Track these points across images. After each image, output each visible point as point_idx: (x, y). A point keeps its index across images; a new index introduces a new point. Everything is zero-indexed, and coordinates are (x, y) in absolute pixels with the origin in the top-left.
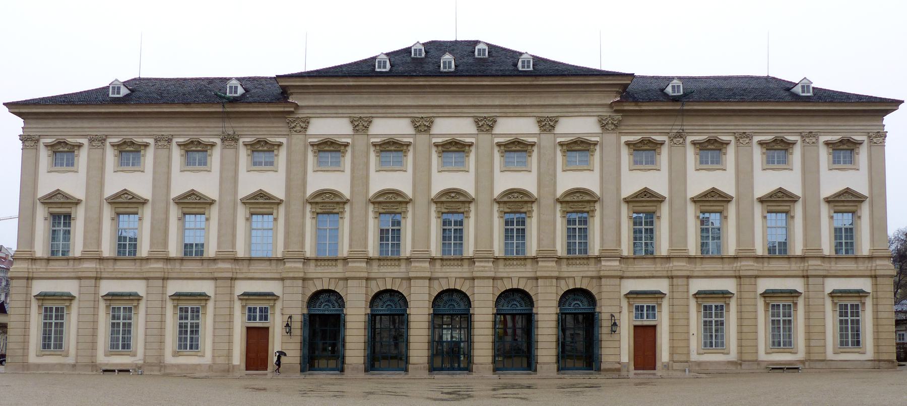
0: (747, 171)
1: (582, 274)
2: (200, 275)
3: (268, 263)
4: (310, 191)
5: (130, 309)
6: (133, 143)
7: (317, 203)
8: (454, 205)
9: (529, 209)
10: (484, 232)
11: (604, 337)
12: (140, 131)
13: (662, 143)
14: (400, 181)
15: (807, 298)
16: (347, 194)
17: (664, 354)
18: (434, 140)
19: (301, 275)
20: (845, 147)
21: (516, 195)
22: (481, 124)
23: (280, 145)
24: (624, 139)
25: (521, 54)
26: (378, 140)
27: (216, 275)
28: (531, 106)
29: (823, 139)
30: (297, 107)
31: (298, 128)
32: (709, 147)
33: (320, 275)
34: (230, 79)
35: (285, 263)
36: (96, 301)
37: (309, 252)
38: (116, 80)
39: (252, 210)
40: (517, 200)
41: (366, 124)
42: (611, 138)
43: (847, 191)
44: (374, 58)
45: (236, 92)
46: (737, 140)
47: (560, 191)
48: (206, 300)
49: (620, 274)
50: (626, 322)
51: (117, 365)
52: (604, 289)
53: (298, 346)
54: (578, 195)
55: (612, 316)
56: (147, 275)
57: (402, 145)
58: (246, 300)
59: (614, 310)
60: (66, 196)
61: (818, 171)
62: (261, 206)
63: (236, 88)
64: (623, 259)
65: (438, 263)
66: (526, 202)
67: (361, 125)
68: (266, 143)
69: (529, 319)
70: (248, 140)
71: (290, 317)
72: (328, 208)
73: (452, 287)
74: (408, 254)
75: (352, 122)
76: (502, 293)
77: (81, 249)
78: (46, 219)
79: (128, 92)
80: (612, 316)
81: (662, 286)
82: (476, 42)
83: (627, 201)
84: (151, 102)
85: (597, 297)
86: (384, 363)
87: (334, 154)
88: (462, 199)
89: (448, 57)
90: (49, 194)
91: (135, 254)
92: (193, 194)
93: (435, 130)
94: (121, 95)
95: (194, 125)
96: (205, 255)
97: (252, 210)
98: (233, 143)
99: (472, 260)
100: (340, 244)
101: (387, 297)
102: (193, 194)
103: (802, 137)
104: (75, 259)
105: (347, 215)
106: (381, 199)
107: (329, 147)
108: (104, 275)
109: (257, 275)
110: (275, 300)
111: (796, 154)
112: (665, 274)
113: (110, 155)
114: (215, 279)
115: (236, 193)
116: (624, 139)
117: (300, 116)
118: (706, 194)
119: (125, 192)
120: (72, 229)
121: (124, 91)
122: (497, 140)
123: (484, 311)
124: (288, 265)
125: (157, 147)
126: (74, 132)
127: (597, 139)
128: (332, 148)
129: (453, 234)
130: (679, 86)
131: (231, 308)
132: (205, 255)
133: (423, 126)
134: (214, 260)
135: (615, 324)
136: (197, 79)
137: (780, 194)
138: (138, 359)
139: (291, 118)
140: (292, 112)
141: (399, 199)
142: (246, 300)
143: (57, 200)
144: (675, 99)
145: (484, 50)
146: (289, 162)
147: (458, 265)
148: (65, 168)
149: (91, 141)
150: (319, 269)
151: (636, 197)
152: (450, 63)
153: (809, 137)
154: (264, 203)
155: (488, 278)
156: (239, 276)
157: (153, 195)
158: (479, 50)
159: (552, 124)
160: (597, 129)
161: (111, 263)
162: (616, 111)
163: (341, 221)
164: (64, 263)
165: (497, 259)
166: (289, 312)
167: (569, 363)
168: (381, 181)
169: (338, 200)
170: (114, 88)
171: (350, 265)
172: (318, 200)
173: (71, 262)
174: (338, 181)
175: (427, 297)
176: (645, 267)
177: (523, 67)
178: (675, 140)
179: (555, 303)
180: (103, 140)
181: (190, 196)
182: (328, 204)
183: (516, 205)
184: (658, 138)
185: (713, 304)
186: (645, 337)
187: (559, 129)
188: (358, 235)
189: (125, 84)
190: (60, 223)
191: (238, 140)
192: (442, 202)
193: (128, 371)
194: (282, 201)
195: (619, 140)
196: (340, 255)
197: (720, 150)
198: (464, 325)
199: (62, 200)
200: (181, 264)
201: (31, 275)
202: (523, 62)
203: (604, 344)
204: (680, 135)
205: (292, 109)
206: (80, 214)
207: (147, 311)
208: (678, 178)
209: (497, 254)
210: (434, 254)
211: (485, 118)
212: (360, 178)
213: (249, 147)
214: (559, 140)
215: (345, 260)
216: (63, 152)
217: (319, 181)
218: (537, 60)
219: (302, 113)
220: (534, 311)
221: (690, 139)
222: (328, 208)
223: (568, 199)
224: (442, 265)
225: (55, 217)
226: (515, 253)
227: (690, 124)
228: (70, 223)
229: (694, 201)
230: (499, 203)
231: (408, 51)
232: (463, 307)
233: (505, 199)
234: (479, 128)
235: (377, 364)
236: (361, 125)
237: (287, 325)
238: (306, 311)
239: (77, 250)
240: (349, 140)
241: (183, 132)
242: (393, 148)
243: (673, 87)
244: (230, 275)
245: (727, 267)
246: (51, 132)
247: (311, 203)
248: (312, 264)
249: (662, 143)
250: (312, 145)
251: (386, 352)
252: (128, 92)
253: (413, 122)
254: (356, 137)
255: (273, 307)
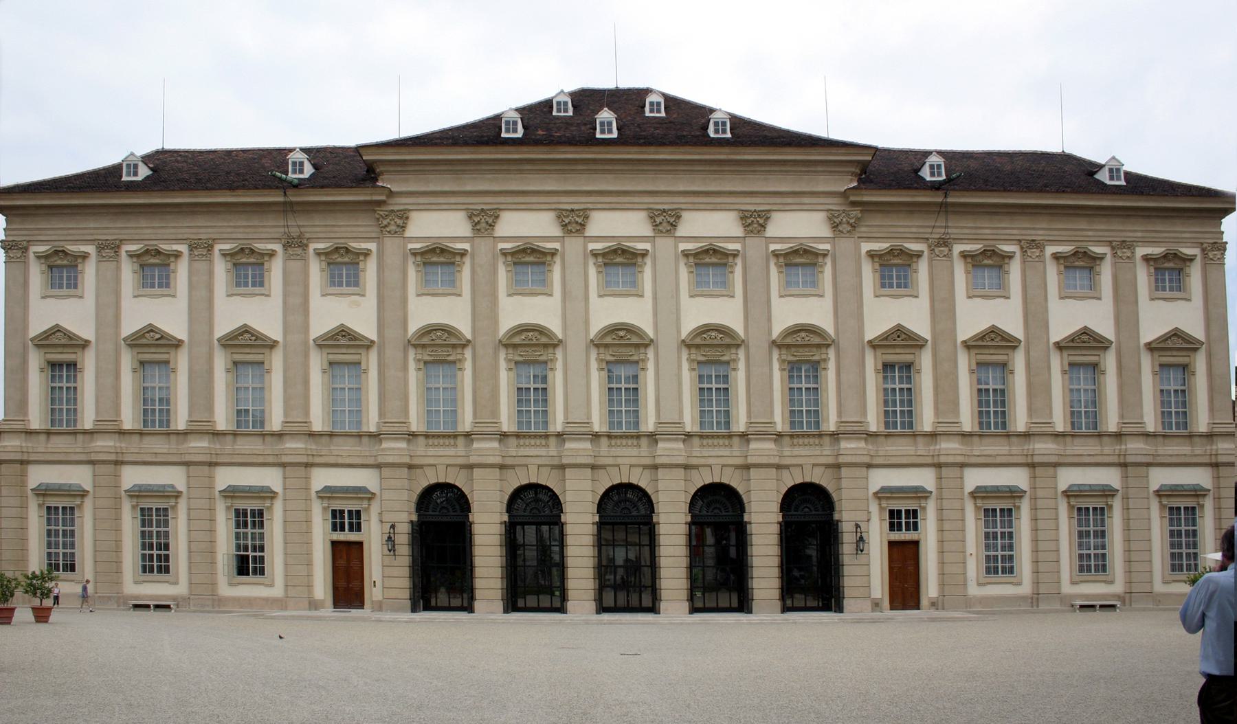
0: (1039, 301)
1: (813, 461)
2: (261, 460)
3: (357, 439)
4: (413, 327)
5: (166, 510)
6: (158, 252)
7: (424, 346)
8: (622, 350)
9: (733, 356)
10: (668, 394)
11: (846, 559)
12: (171, 236)
13: (919, 255)
14: (542, 310)
15: (1126, 498)
16: (466, 330)
17: (930, 588)
18: (592, 246)
19: (407, 460)
20: (1171, 265)
21: (713, 334)
22: (658, 220)
23: (367, 254)
24: (866, 247)
25: (712, 111)
26: (508, 245)
27: (285, 459)
28: (731, 193)
29: (1141, 251)
30: (391, 194)
31: (393, 228)
32: (986, 262)
33: (432, 461)
34: (291, 150)
35: (381, 441)
36: (118, 499)
37: (416, 423)
38: (132, 154)
39: (331, 357)
40: (715, 342)
41: (490, 221)
42: (845, 244)
43: (1176, 334)
44: (498, 118)
45: (301, 171)
46: (1024, 251)
47: (777, 330)
48: (272, 498)
49: (866, 460)
50: (878, 536)
51: (152, 597)
52: (844, 483)
53: (406, 572)
54: (803, 334)
55: (857, 526)
56: (188, 458)
57: (544, 254)
58: (329, 498)
59: (860, 516)
60: (69, 336)
61: (1136, 302)
62: (344, 351)
63: (302, 164)
64: (871, 436)
65: (604, 441)
66: (729, 346)
67: (483, 222)
68: (347, 250)
69: (741, 531)
70: (321, 246)
71: (393, 527)
72: (441, 353)
73: (625, 481)
74: (559, 428)
75: (470, 217)
76: (699, 490)
77: (93, 417)
78: (42, 370)
79: (149, 172)
80: (857, 526)
81: (924, 478)
82: (647, 91)
83: (873, 345)
84: (185, 185)
85: (835, 496)
86: (531, 601)
87: (446, 269)
88: (635, 340)
89: (606, 115)
90: (45, 332)
91: (168, 426)
92: (247, 332)
93: (593, 229)
94: (140, 178)
95: (245, 224)
96: (267, 428)
97: (331, 357)
98: (299, 251)
99: (653, 437)
100: (459, 411)
101: (531, 494)
102: (247, 332)
103: (1113, 248)
104: (85, 432)
105: (468, 365)
106: (517, 340)
107: (439, 258)
108: (127, 458)
109: (340, 461)
110: (370, 499)
111: (1106, 273)
112: (929, 460)
113: (128, 272)
114: (283, 465)
115: (306, 328)
116: (866, 247)
117: (396, 208)
118: (982, 336)
119: (151, 329)
120: (79, 385)
121: (144, 172)
122: (683, 246)
123: (674, 518)
124: (385, 445)
125: (192, 259)
126: (79, 237)
127: (827, 247)
128: (442, 259)
129: (623, 395)
130: (939, 166)
131: (308, 511)
132: (267, 428)
133: (573, 223)
134: (280, 435)
135: (861, 539)
136: (244, 151)
137: (1085, 337)
138: (181, 589)
139: (381, 211)
140: (380, 203)
141: (544, 340)
142: (329, 498)
143: (57, 342)
144: (936, 187)
145: (659, 104)
146: (381, 283)
147: (633, 446)
148: (65, 291)
149: (100, 248)
150: (431, 452)
151: (886, 339)
152: (610, 124)
153: (1122, 247)
154: (348, 346)
155: (677, 466)
156: (318, 460)
157: (191, 333)
158: (652, 104)
159: (761, 221)
160: (826, 232)
161: (136, 438)
162: (854, 204)
163: (459, 373)
164: (69, 438)
165: (689, 436)
166: (389, 518)
167: (799, 600)
168: (515, 311)
169: (454, 341)
170: (128, 166)
171: (476, 445)
172: (425, 340)
173: (80, 437)
174: (454, 312)
175: (589, 496)
176: (900, 448)
177: (716, 131)
178: (937, 250)
179: (775, 507)
180: (116, 248)
181: (241, 334)
182: (439, 346)
183: (713, 347)
184: (914, 247)
185: (998, 509)
186: (905, 559)
187: (772, 230)
188: (486, 401)
189: (146, 159)
190: (61, 377)
191: (307, 246)
192: (607, 346)
193: (168, 607)
194: (372, 342)
195: (858, 249)
196: (460, 429)
197: (1000, 267)
198: (645, 540)
199: (63, 342)
200: (234, 442)
201: (25, 458)
202: (716, 124)
203: (847, 570)
204: (945, 242)
205: (383, 198)
206: (89, 363)
207: (189, 515)
208: (943, 310)
209: (688, 429)
210: (596, 428)
211: (664, 211)
212: (485, 307)
213: (323, 258)
214: (773, 247)
215: (468, 435)
216: (63, 269)
217: (425, 311)
218: (738, 122)
219: (398, 204)
220: (746, 518)
221: (958, 248)
222: (441, 353)
223: (789, 341)
224: (610, 446)
225: (54, 366)
226: (717, 427)
227: (958, 226)
228: (75, 376)
229: (967, 345)
230: (689, 347)
231: (547, 105)
232: (643, 512)
233: (698, 341)
234: (656, 226)
235: (521, 603)
236: (483, 222)
237: (389, 538)
238: (414, 518)
239: (87, 420)
240: (467, 246)
241: (227, 234)
242: (531, 259)
243: (932, 167)
244: (304, 459)
245: (1016, 449)
246: (47, 235)
247: (415, 346)
248: (421, 440)
249: (919, 255)
250: (414, 254)
251: (534, 583)
252: (149, 172)
253: (559, 217)
254: (477, 240)
255: (367, 509)
